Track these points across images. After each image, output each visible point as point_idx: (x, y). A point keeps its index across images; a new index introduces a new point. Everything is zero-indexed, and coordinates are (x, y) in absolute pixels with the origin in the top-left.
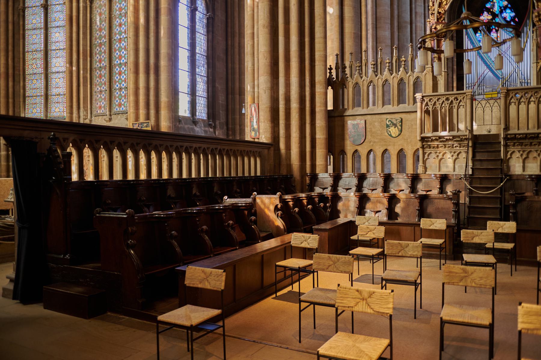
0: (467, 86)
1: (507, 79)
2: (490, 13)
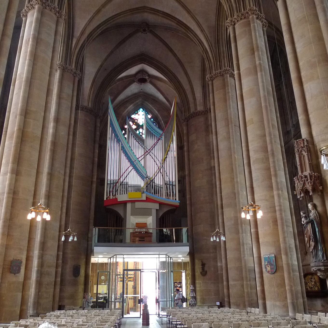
0: (109, 183)
1: (151, 179)
2: (134, 123)
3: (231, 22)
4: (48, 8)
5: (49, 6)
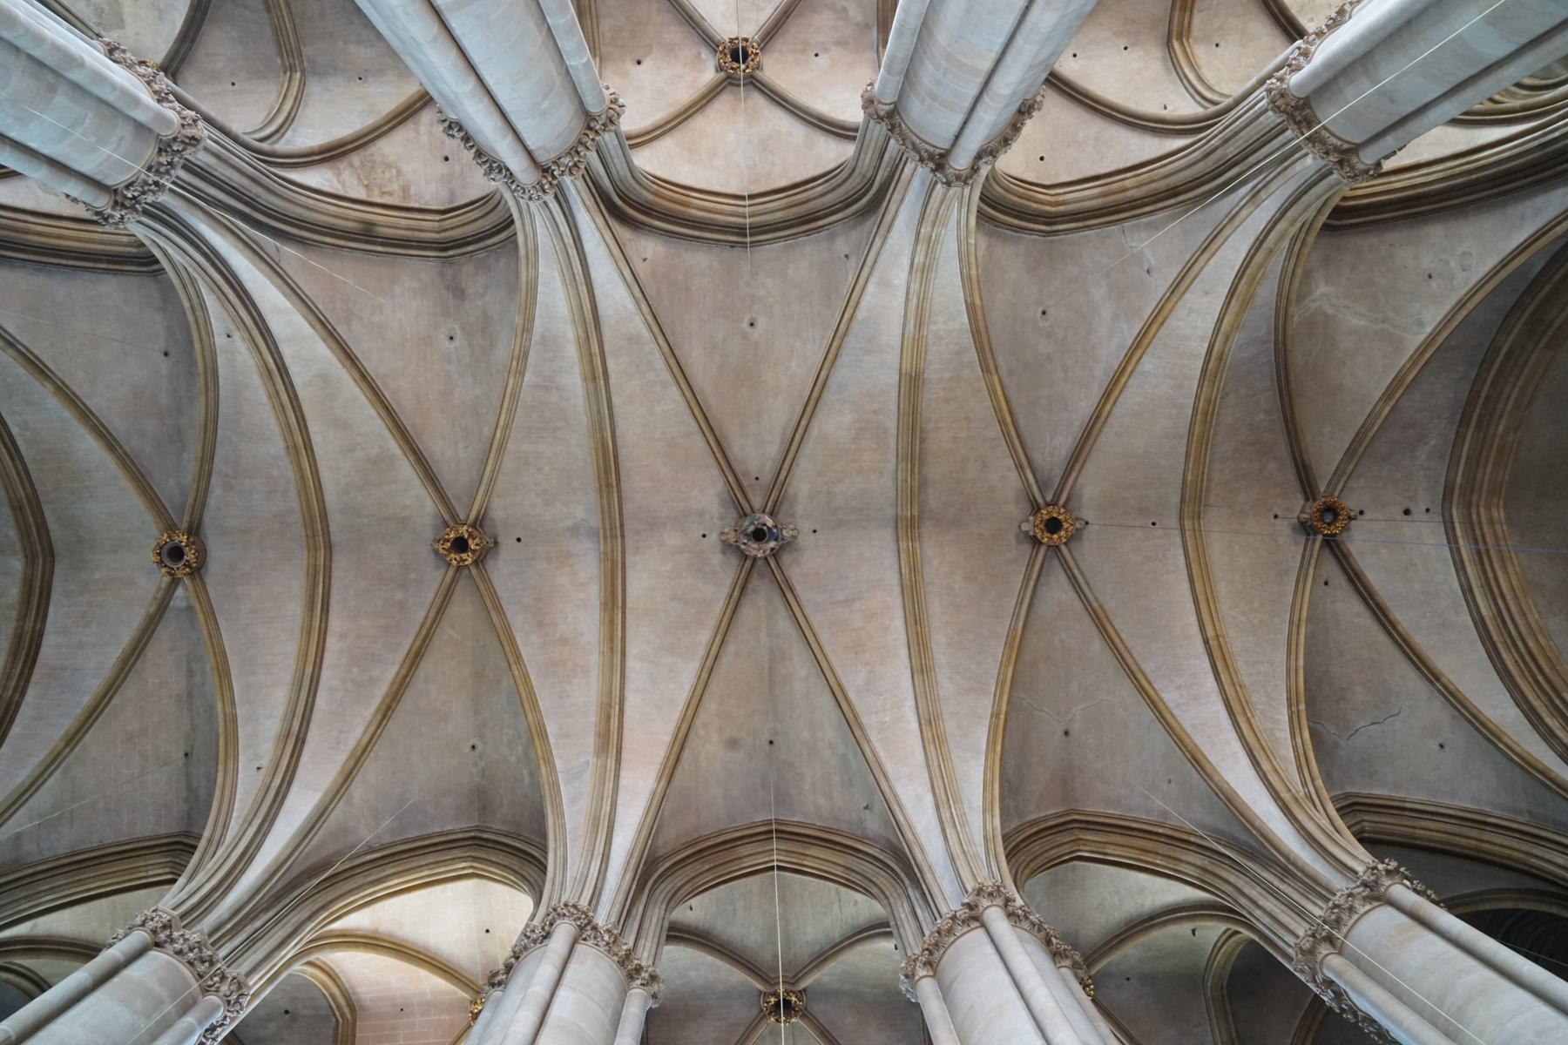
3: (164, 927)
4: (163, 160)
5: (169, 164)
